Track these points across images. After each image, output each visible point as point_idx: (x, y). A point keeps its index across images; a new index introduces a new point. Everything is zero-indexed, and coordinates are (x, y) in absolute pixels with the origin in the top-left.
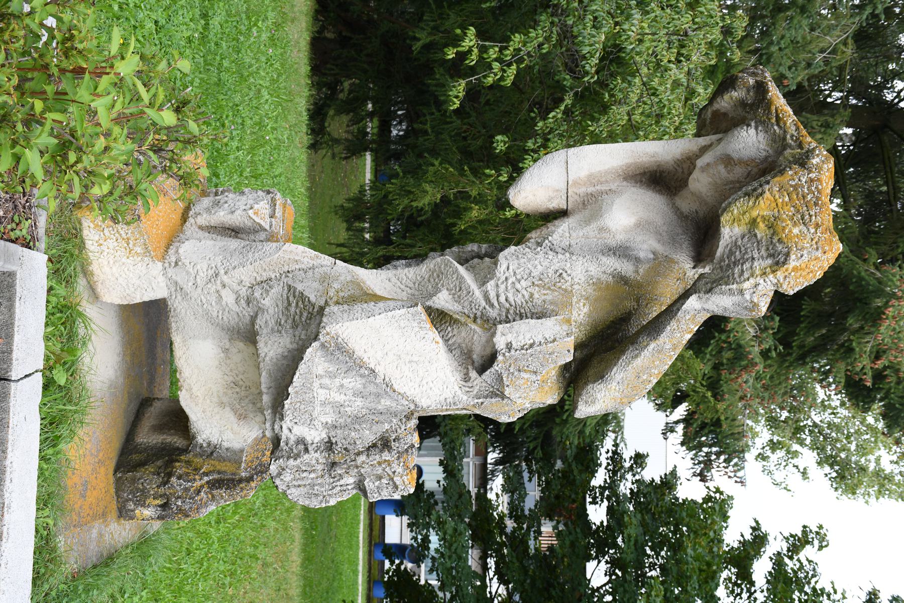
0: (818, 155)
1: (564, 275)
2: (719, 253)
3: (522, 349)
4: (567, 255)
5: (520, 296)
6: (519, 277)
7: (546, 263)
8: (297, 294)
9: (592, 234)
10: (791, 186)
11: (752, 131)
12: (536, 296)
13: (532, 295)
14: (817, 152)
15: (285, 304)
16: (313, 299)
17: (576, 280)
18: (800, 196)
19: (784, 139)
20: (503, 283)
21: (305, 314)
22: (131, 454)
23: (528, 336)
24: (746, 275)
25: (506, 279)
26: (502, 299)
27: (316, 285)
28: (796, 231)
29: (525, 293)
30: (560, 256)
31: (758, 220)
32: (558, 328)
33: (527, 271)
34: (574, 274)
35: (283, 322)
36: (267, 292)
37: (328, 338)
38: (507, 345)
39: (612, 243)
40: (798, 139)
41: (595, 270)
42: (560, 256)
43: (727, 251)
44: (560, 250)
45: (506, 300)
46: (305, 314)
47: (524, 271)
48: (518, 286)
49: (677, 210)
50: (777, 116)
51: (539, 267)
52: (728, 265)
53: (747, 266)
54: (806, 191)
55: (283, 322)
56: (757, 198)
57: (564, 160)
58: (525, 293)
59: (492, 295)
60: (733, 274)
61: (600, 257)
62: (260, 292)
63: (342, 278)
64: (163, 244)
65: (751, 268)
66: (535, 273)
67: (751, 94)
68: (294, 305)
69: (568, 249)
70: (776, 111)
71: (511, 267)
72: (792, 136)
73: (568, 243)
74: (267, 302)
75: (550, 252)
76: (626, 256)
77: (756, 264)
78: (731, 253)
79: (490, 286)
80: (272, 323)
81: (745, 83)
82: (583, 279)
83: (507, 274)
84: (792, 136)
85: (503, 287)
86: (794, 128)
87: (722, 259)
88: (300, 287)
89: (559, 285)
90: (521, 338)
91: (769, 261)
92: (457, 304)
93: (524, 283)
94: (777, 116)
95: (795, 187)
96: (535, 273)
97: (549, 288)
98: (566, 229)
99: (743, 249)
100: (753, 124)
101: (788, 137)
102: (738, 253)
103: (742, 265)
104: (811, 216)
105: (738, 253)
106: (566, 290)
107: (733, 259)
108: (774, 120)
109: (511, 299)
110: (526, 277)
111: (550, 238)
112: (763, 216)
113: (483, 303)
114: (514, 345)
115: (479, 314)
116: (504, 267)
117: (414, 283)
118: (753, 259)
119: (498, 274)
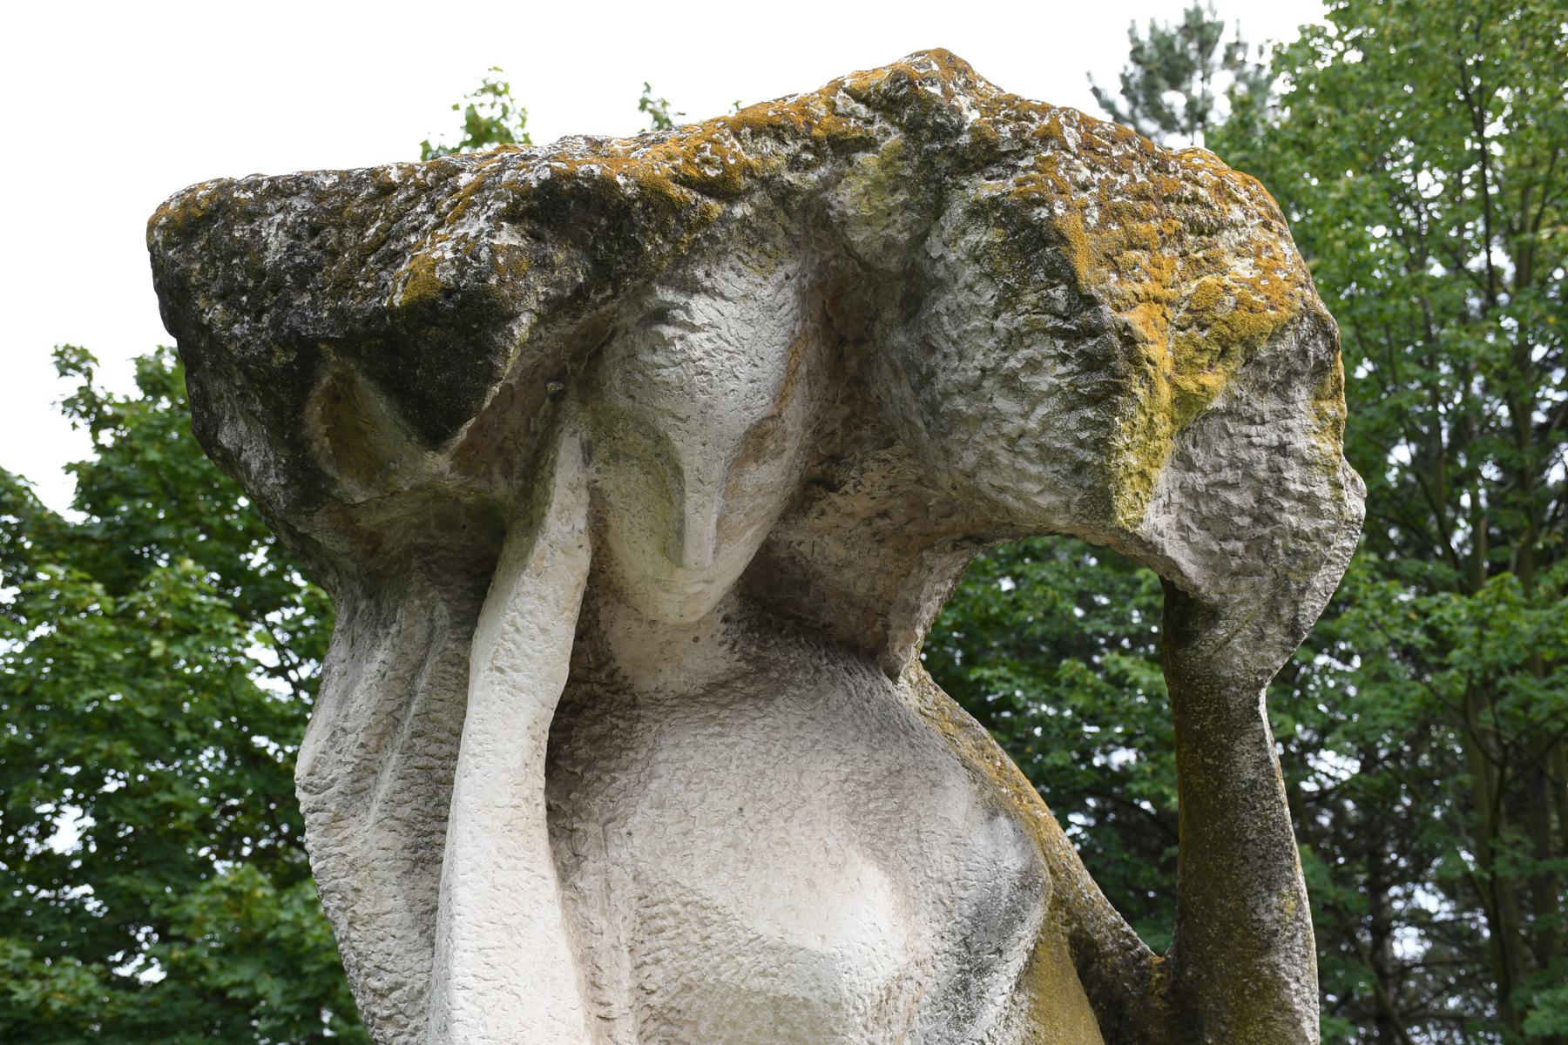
10: (1102, 224)
11: (702, 309)
14: (936, 90)
18: (1140, 206)
19: (784, 195)
24: (1323, 490)
31: (1190, 385)
39: (944, 971)
40: (816, 147)
43: (1198, 536)
49: (717, 697)
50: (708, 188)
52: (1254, 544)
53: (1293, 476)
54: (1123, 180)
56: (1135, 360)
60: (1297, 534)
65: (1306, 463)
67: (560, 257)
70: (686, 182)
72: (794, 163)
76: (1009, 925)
77: (1300, 443)
81: (512, 265)
84: (794, 163)
86: (768, 145)
87: (1216, 564)
91: (1301, 395)
94: (708, 188)
95: (1113, 214)
99: (1228, 475)
100: (668, 295)
101: (789, 177)
102: (1234, 498)
103: (1285, 493)
104: (1195, 199)
105: (1234, 498)
108: (716, 208)
118: (1282, 449)
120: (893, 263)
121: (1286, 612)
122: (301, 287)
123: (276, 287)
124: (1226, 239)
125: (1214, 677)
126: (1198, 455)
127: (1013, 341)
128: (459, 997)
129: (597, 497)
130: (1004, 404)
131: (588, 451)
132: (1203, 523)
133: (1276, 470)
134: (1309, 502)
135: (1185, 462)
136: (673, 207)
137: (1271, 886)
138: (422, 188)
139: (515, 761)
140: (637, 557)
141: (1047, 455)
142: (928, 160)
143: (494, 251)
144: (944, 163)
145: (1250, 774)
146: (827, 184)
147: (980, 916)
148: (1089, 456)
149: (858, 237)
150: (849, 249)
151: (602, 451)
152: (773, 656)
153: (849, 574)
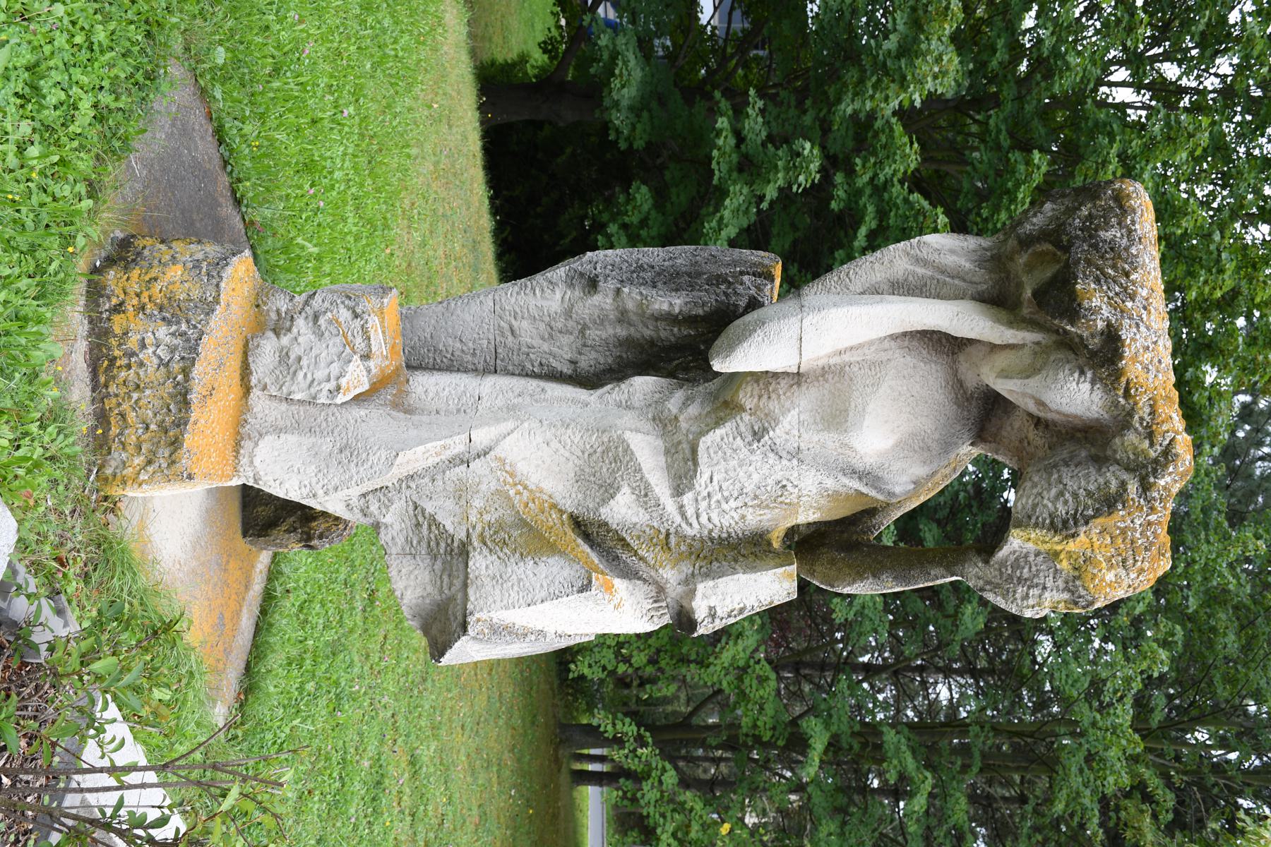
0: (1170, 474)
1: (789, 487)
2: (1002, 554)
3: (729, 616)
4: (795, 462)
5: (727, 517)
6: (726, 494)
7: (765, 471)
8: (427, 515)
9: (830, 444)
10: (1118, 528)
11: (1086, 386)
12: (749, 517)
13: (743, 517)
14: (1171, 469)
15: (414, 521)
16: (450, 528)
17: (805, 492)
18: (1128, 541)
19: (1130, 414)
20: (704, 498)
21: (443, 545)
22: (255, 507)
23: (737, 599)
24: (1031, 602)
25: (709, 495)
26: (704, 519)
27: (450, 504)
28: (1110, 576)
29: (734, 514)
30: (784, 462)
31: (1062, 556)
32: (776, 586)
33: (738, 486)
34: (802, 485)
35: (415, 542)
36: (387, 507)
37: (479, 627)
38: (710, 608)
39: (859, 466)
40: (1148, 426)
41: (830, 483)
42: (784, 462)
43: (1012, 558)
44: (784, 454)
45: (709, 519)
46: (443, 545)
47: (733, 484)
48: (725, 506)
49: (957, 385)
50: (1127, 390)
51: (756, 477)
52: (1010, 577)
53: (1036, 591)
54: (1138, 535)
55: (415, 542)
56: (1067, 537)
57: (796, 337)
58: (734, 514)
59: (690, 512)
60: (1015, 592)
61: (840, 476)
62: (377, 505)
63: (483, 487)
64: (229, 454)
65: (1040, 596)
66: (749, 488)
67: (1096, 341)
68: (425, 526)
69: (796, 454)
70: (1128, 383)
71: (715, 479)
72: (1142, 419)
73: (796, 445)
74: (388, 519)
75: (771, 455)
77: (1047, 594)
78: (1016, 565)
79: (688, 498)
80: (400, 540)
81: (1090, 327)
82: (815, 491)
83: (710, 489)
84: (1142, 419)
85: (703, 505)
86: (1147, 410)
87: (1003, 563)
88: (429, 508)
89: (780, 499)
90: (728, 601)
91: (1066, 596)
92: (642, 511)
93: (733, 504)
94: (1127, 390)
95: (1124, 532)
96: (749, 488)
97: (767, 507)
98: (795, 422)
99: (1034, 569)
100: (1089, 375)
101: (1136, 417)
102: (1026, 570)
103: (1029, 588)
104: (1136, 561)
105: (1026, 570)
106: (790, 504)
107: (1018, 574)
108: (1121, 392)
109: (716, 520)
110: (736, 495)
111: (771, 433)
112: (1068, 552)
113: (678, 519)
114: (719, 613)
115: (672, 530)
116: (706, 476)
117: (583, 452)
118: (1045, 588)
119: (697, 486)
120: (1109, 453)
121: (988, 587)
122: (1090, 246)
123: (1091, 237)
124: (1123, 573)
125: (965, 561)
126: (1040, 558)
127: (1075, 495)
128: (845, 310)
129: (1023, 346)
130: (1054, 492)
131: (1038, 343)
132: (1017, 559)
133: (1037, 585)
134: (1026, 597)
135: (1037, 554)
136: (1118, 378)
137: (895, 578)
138: (1126, 289)
139: (925, 321)
140: (1002, 360)
141: (1035, 506)
142: (1145, 466)
143: (1095, 320)
144: (1144, 473)
145: (933, 573)
146: (1136, 430)
147: (878, 478)
148: (1033, 521)
149: (1117, 441)
150: (1114, 437)
151: (1037, 349)
152: (974, 403)
153: (1009, 429)
